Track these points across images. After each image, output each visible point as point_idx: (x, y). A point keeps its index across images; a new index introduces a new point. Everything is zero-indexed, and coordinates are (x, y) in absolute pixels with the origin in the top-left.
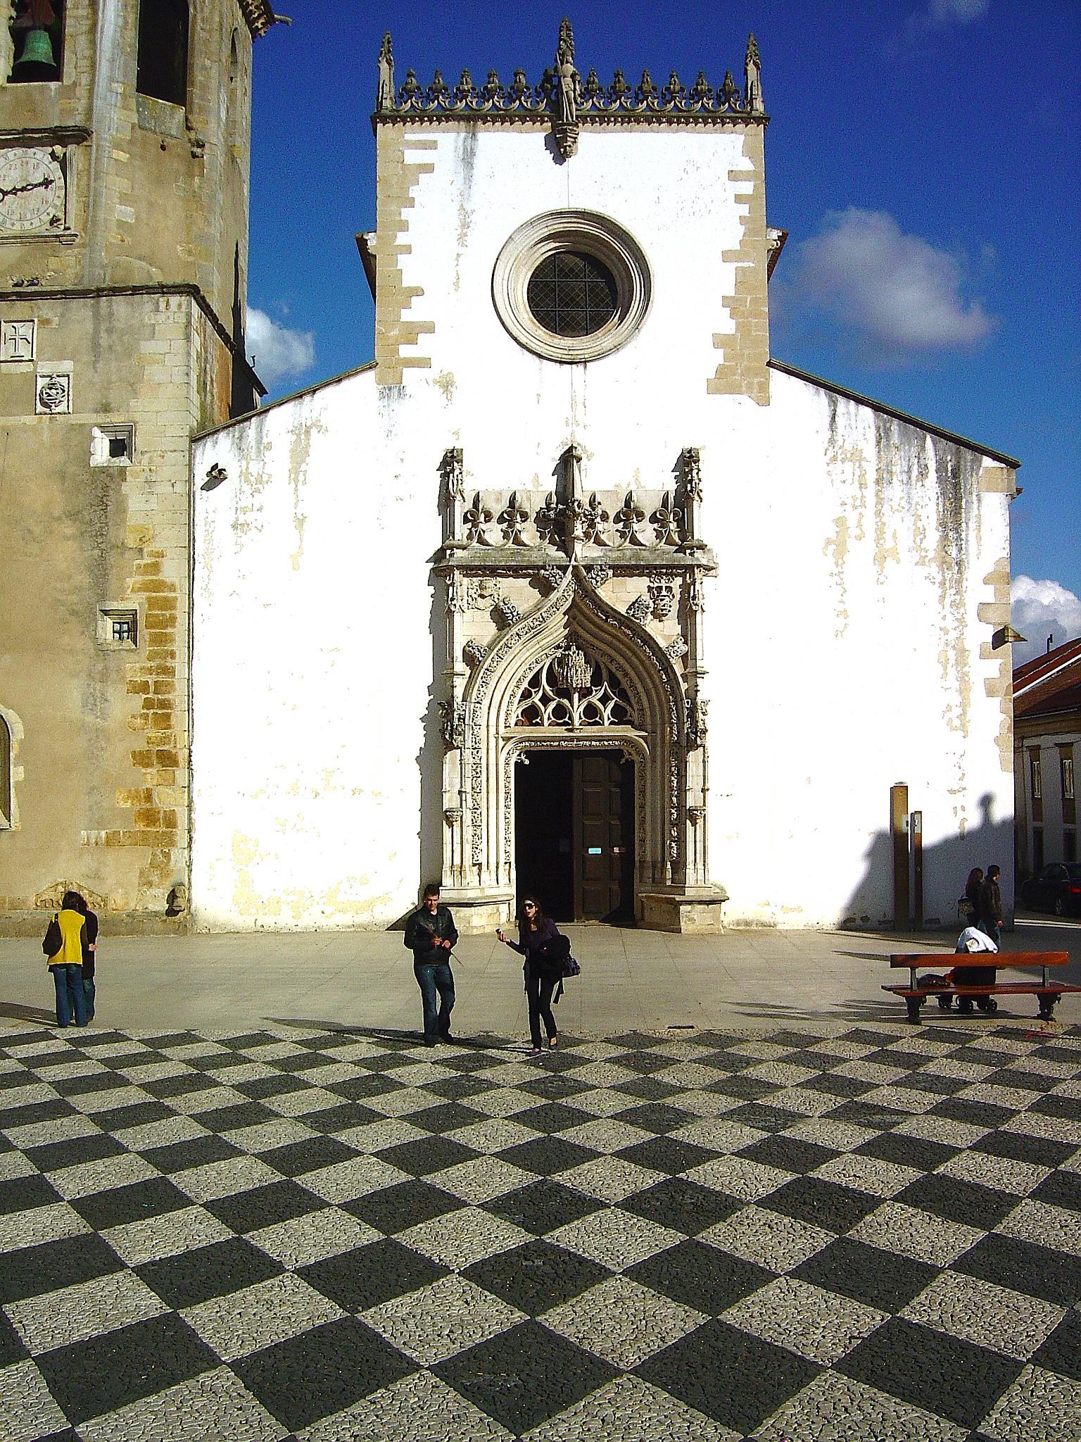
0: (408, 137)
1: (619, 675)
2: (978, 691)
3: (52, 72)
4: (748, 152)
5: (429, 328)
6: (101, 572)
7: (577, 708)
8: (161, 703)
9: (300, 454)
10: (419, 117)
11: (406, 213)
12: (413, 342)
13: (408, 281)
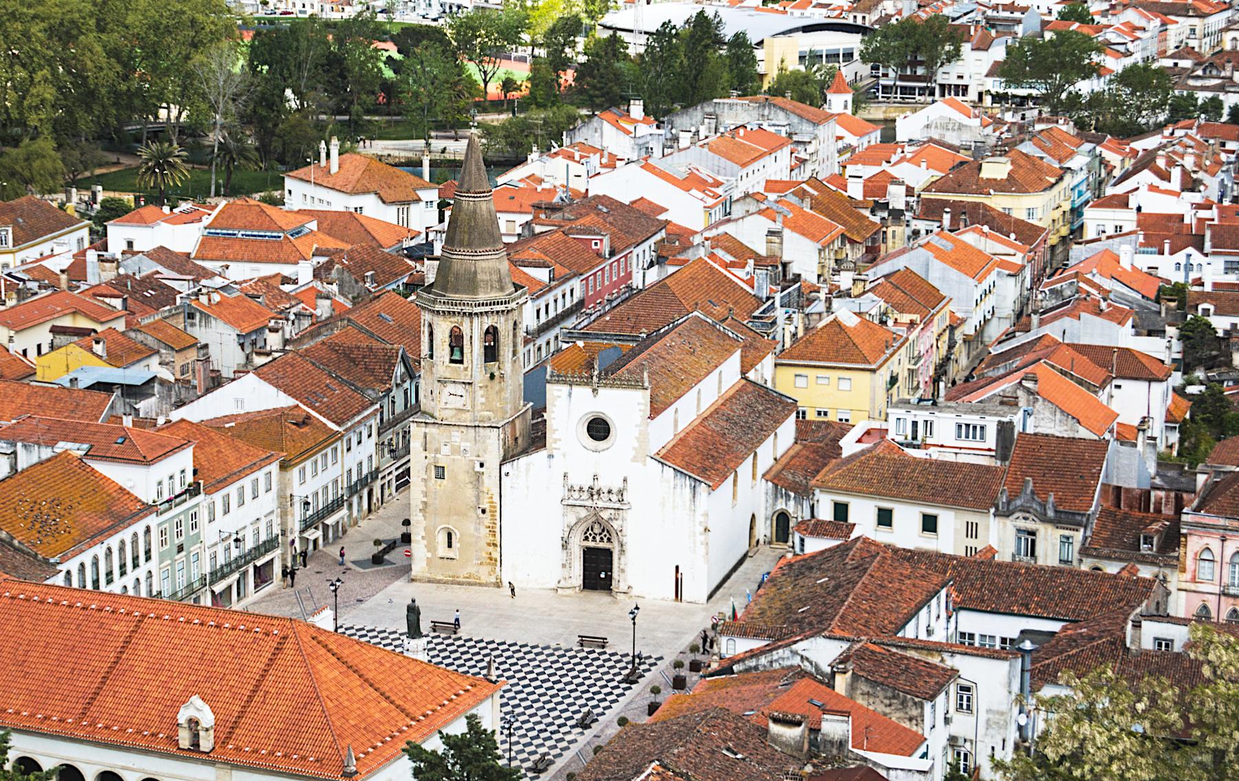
2: (698, 544)
3: (461, 362)
4: (644, 398)
6: (478, 497)
7: (598, 538)
8: (495, 531)
9: (528, 470)
10: (558, 382)
13: (555, 427)
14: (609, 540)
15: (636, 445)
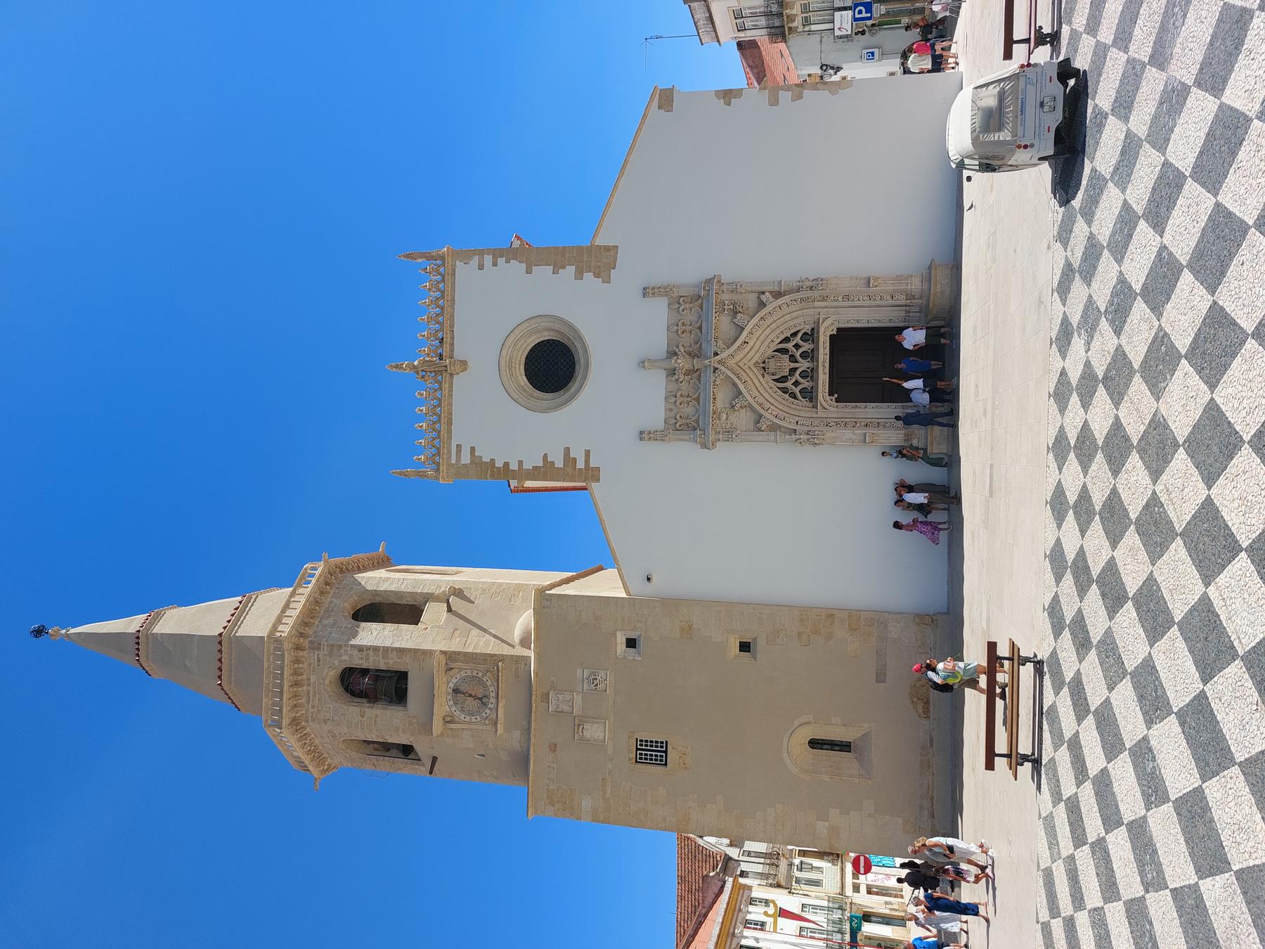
0: (453, 461)
1: (782, 337)
5: (567, 450)
7: (804, 365)
11: (499, 464)
12: (575, 459)
13: (541, 464)
14: (806, 337)
15: (571, 269)
